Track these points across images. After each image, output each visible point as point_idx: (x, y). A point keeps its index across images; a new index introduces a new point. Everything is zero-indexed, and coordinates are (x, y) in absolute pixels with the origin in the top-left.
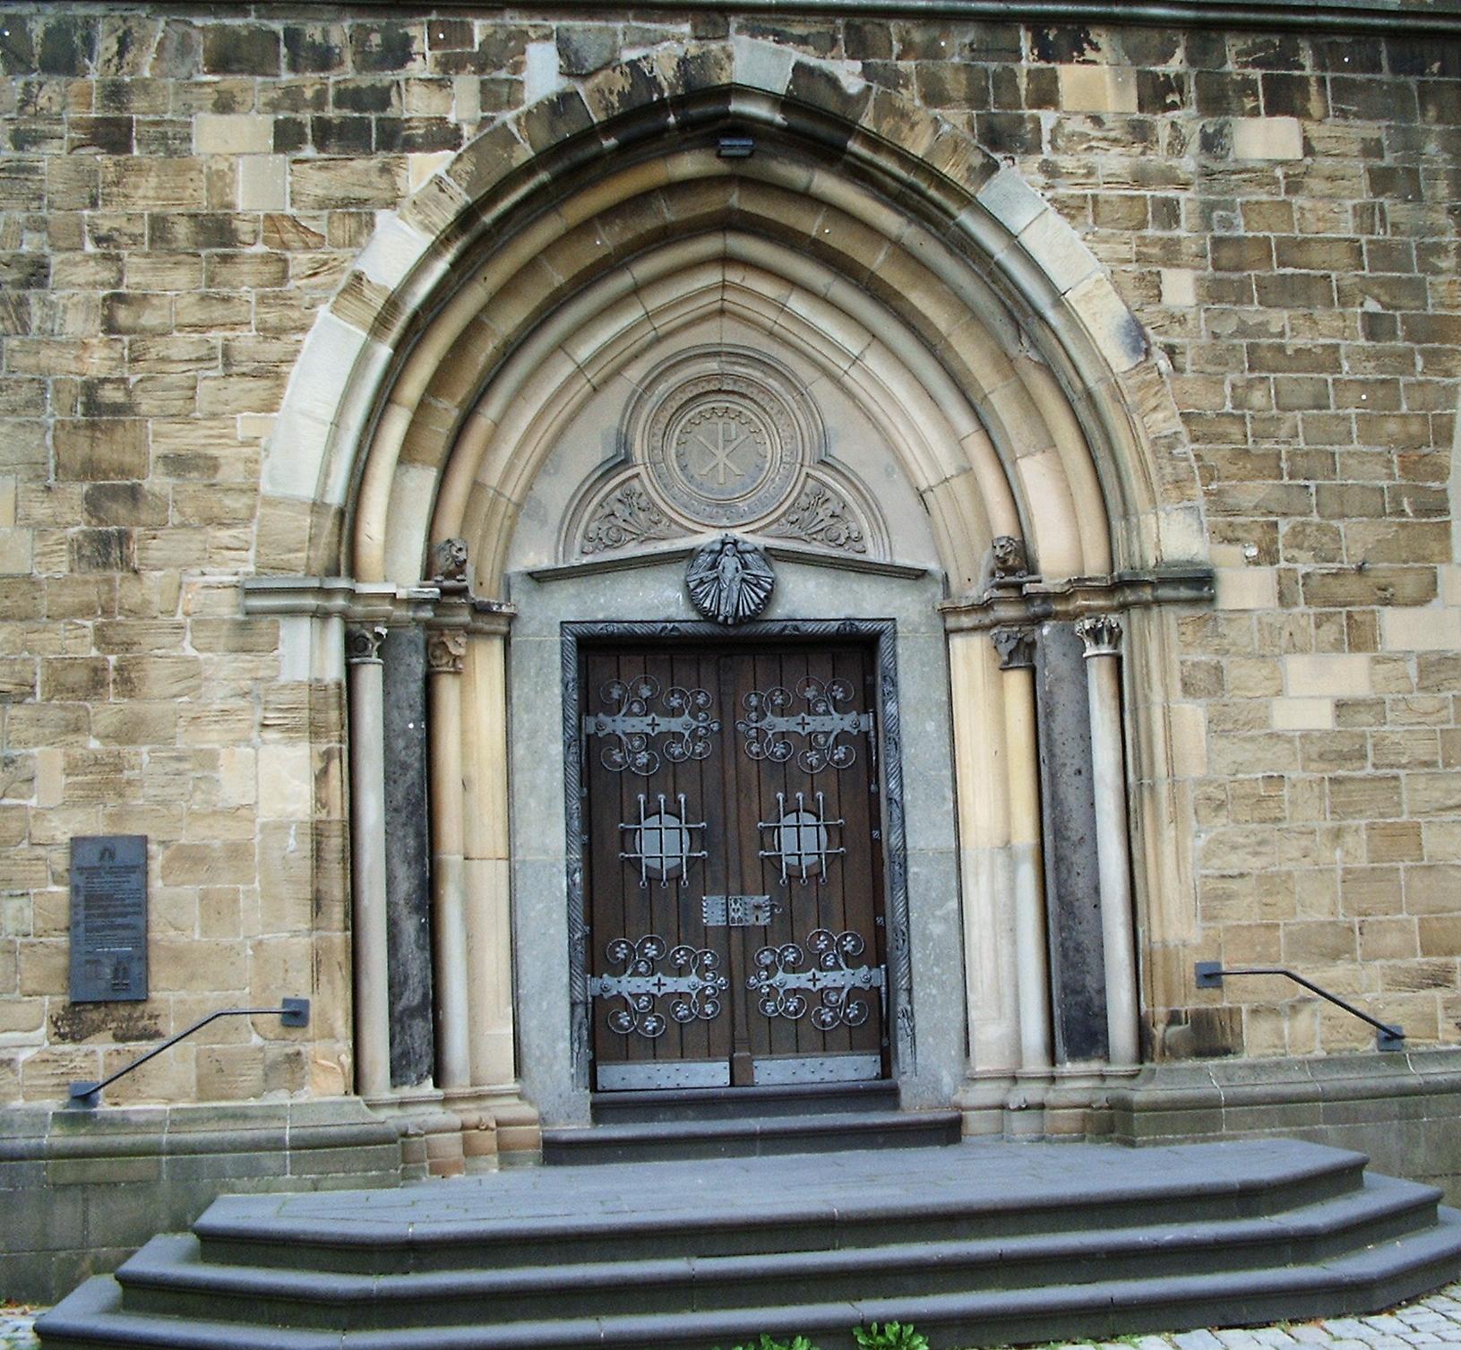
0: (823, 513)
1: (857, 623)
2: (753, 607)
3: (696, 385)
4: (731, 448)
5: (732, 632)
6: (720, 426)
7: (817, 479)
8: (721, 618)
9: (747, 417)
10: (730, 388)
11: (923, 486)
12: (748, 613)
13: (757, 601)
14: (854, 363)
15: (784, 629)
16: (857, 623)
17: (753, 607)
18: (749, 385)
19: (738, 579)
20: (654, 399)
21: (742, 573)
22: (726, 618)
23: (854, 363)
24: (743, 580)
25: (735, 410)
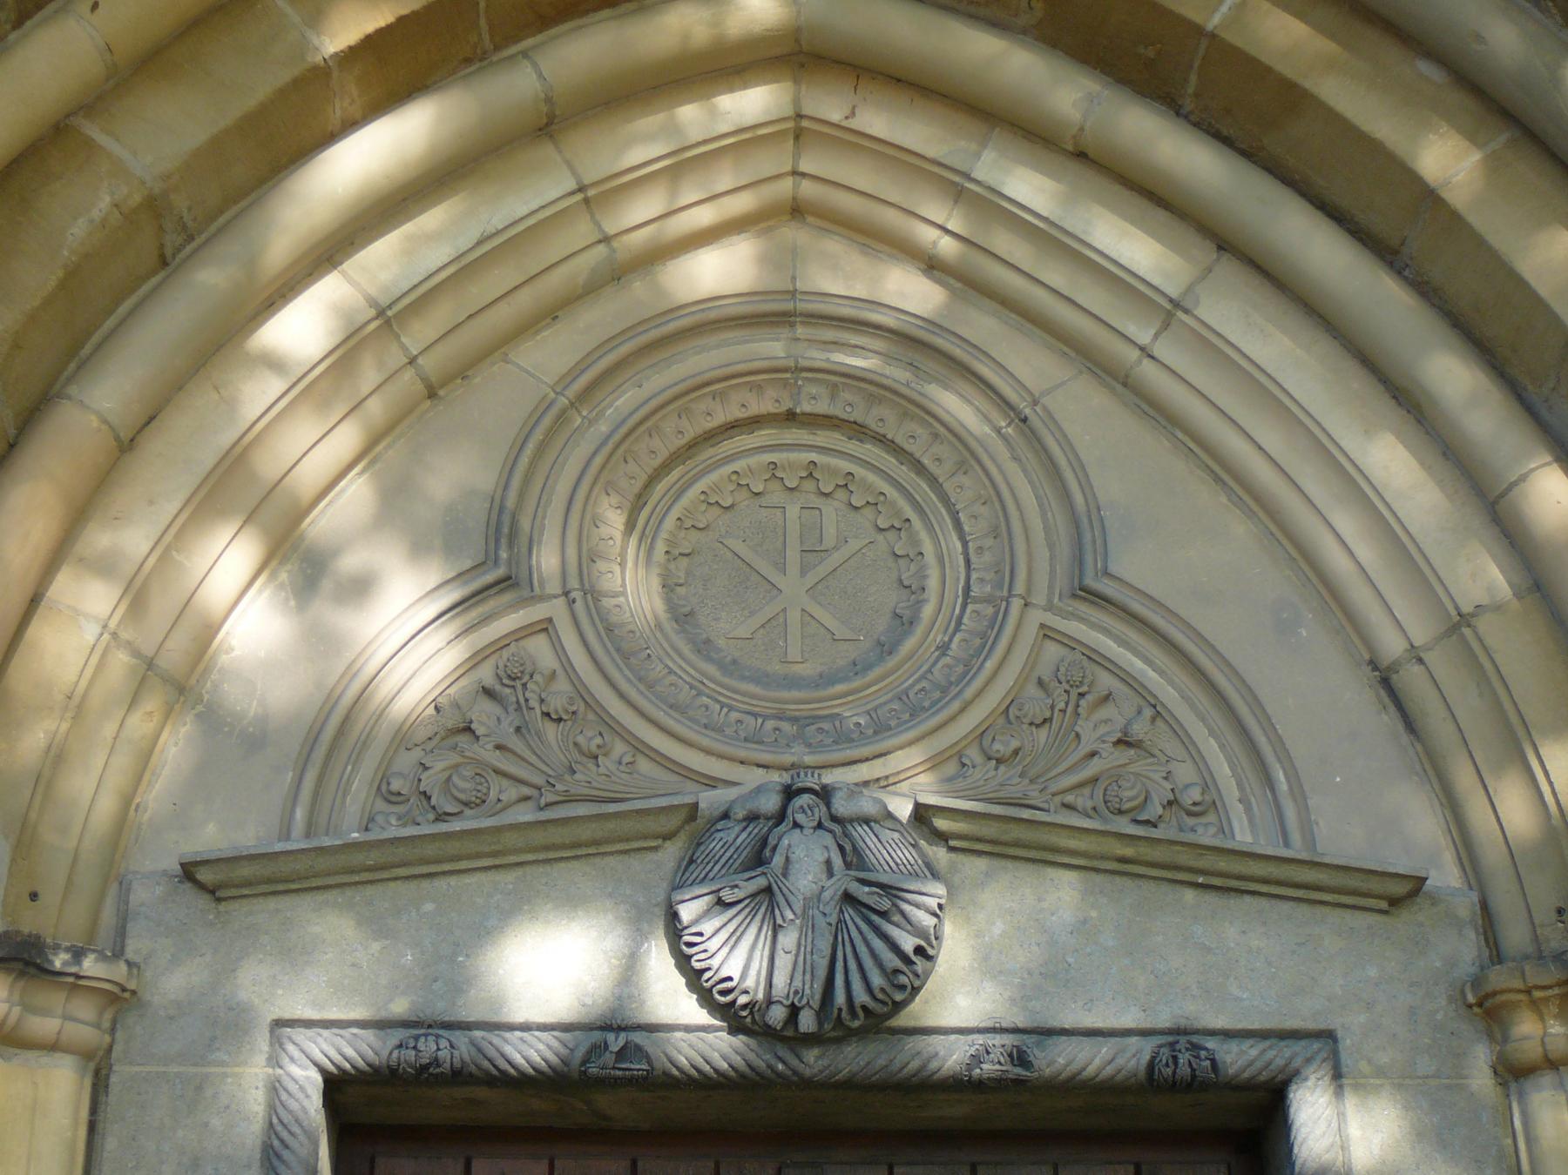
0: (1095, 729)
1: (1211, 1044)
2: (877, 980)
3: (721, 396)
4: (822, 570)
5: (813, 1061)
6: (793, 511)
7: (1069, 642)
8: (777, 1015)
9: (868, 488)
10: (822, 407)
11: (1392, 645)
12: (861, 997)
13: (892, 961)
14: (1166, 325)
15: (976, 1059)
16: (1211, 1044)
17: (877, 980)
18: (872, 400)
19: (833, 889)
20: (603, 428)
21: (844, 881)
22: (794, 1011)
23: (1166, 325)
24: (848, 898)
25: (833, 472)
